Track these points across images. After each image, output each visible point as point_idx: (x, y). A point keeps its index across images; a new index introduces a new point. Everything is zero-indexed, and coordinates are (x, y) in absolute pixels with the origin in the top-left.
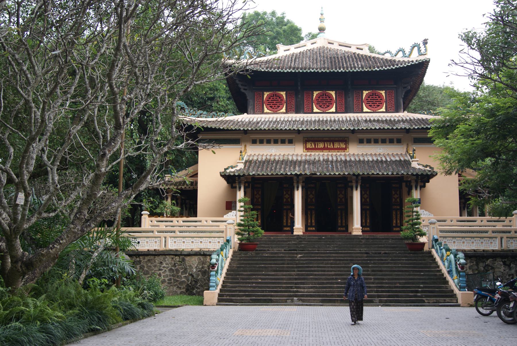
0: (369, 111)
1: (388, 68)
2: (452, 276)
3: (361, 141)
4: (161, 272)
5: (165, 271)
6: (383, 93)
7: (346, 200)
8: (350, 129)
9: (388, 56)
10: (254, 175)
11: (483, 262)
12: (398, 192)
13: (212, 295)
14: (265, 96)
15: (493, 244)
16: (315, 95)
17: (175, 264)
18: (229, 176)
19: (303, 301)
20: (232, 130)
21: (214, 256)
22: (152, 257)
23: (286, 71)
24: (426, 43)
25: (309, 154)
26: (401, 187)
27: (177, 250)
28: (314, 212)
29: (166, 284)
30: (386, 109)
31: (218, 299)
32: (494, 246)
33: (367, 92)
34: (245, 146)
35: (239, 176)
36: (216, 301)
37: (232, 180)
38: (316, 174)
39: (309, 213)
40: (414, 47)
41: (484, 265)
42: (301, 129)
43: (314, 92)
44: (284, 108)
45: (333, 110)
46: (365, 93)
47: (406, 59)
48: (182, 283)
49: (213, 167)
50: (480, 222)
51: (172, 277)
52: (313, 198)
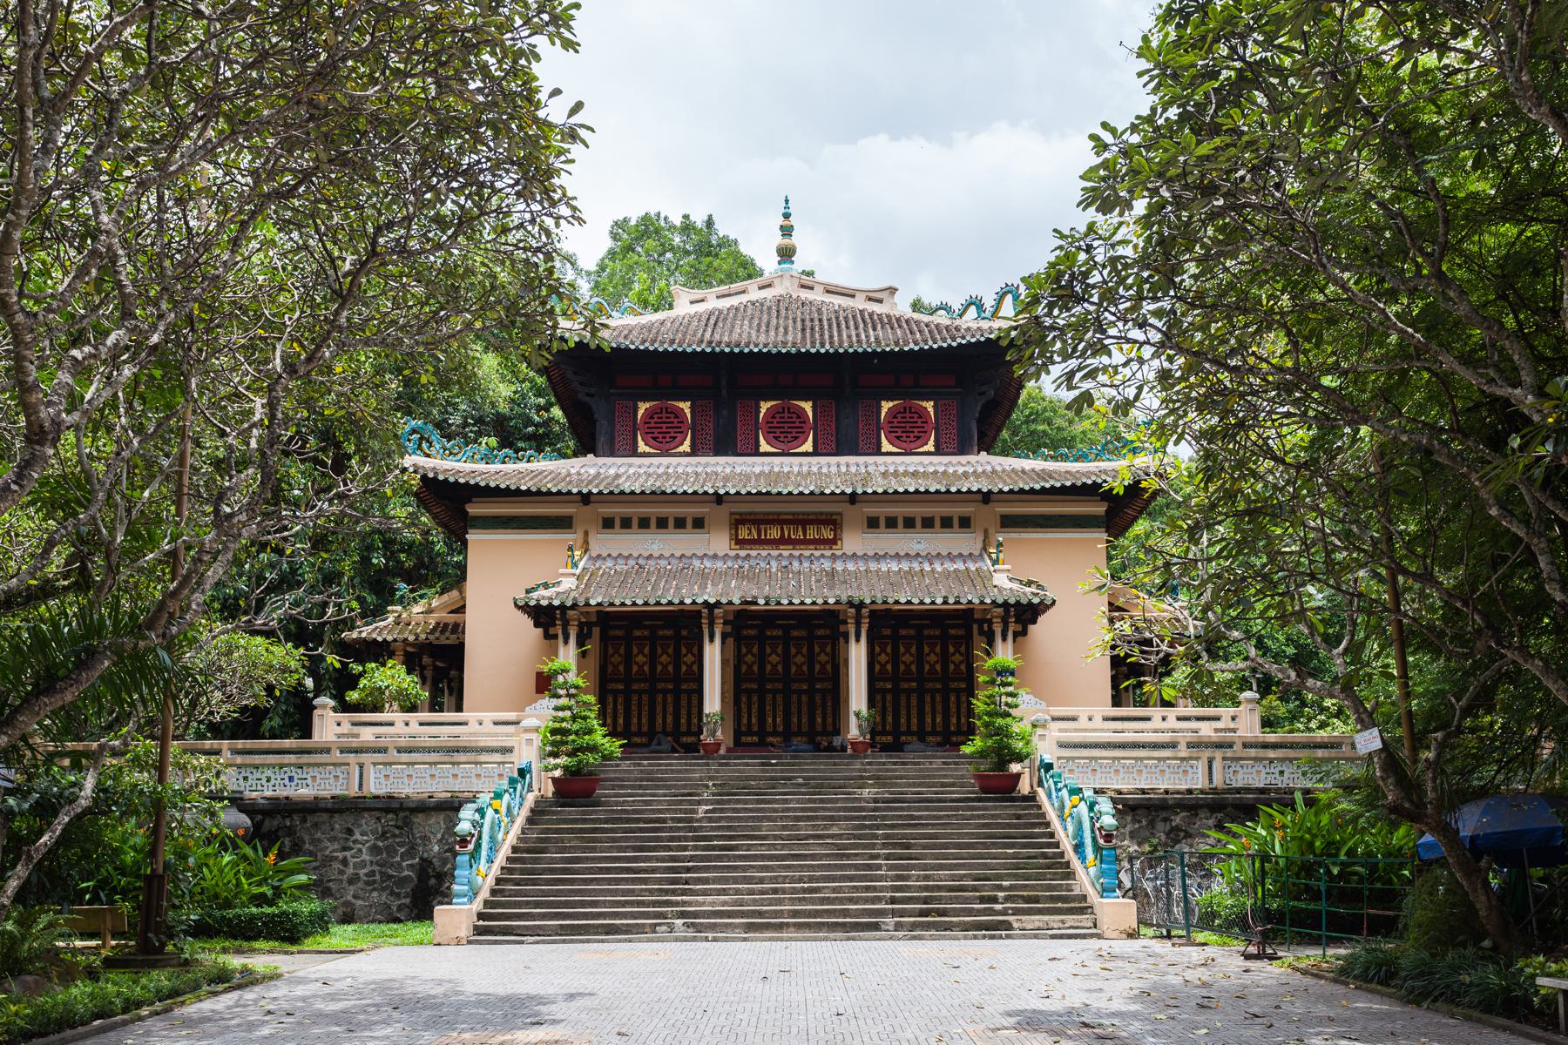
0: (896, 450)
1: (940, 343)
2: (1083, 859)
3: (873, 523)
4: (348, 854)
5: (360, 850)
6: (929, 406)
7: (836, 668)
8: (843, 493)
9: (942, 318)
10: (599, 604)
11: (1166, 820)
12: (963, 649)
13: (456, 915)
14: (641, 412)
15: (1190, 776)
16: (763, 411)
17: (384, 833)
18: (538, 607)
19: (699, 928)
20: (549, 493)
21: (467, 814)
22: (325, 816)
23: (689, 350)
25: (743, 553)
26: (969, 637)
27: (391, 797)
28: (755, 699)
29: (360, 885)
30: (937, 445)
31: (476, 928)
32: (1195, 779)
33: (891, 404)
34: (586, 534)
35: (562, 607)
36: (465, 931)
37: (546, 617)
38: (756, 603)
40: (1005, 294)
41: (1168, 827)
42: (722, 492)
44: (687, 442)
45: (808, 446)
47: (985, 325)
48: (402, 881)
49: (502, 583)
50: (1160, 723)
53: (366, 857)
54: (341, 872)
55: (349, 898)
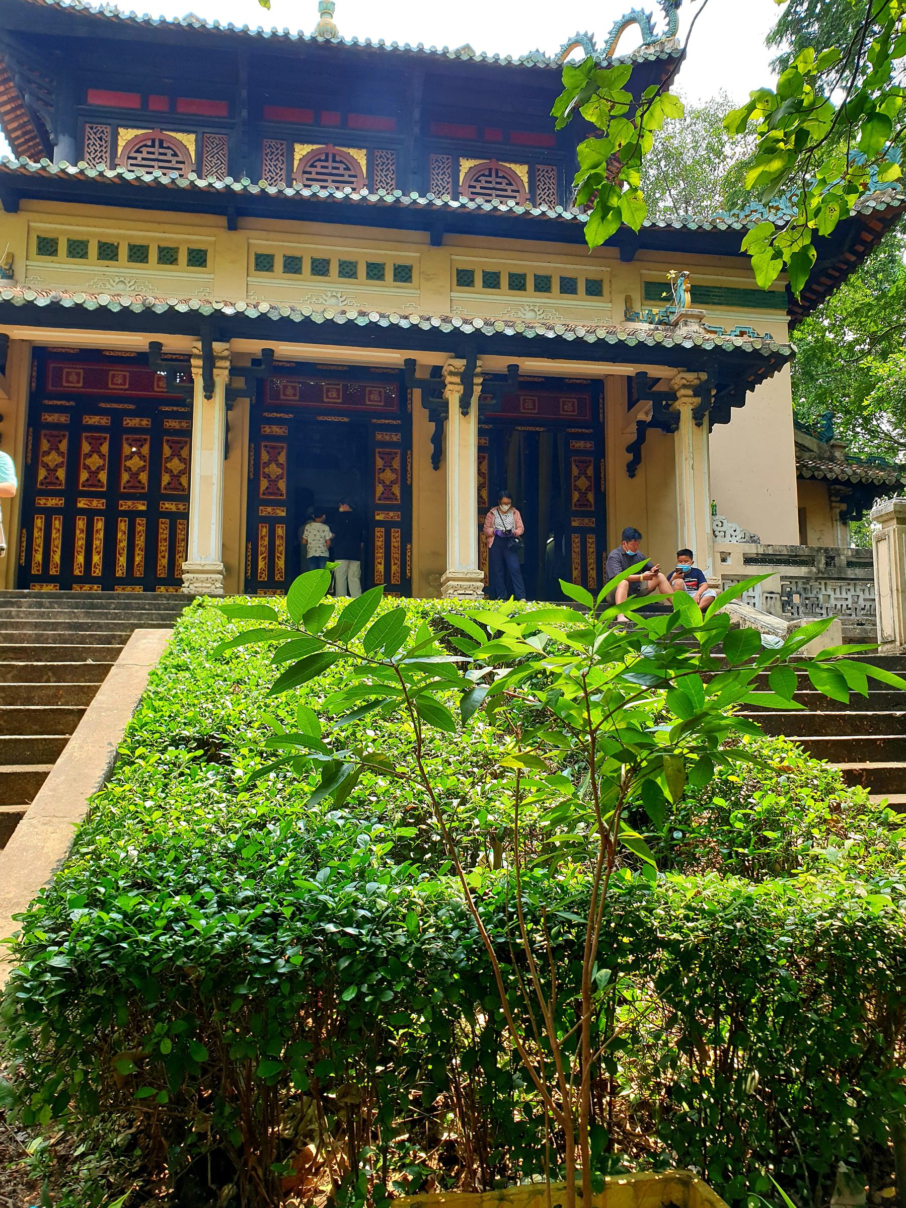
16: (297, 157)
39: (264, 531)
43: (298, 147)
46: (466, 165)
52: (280, 477)
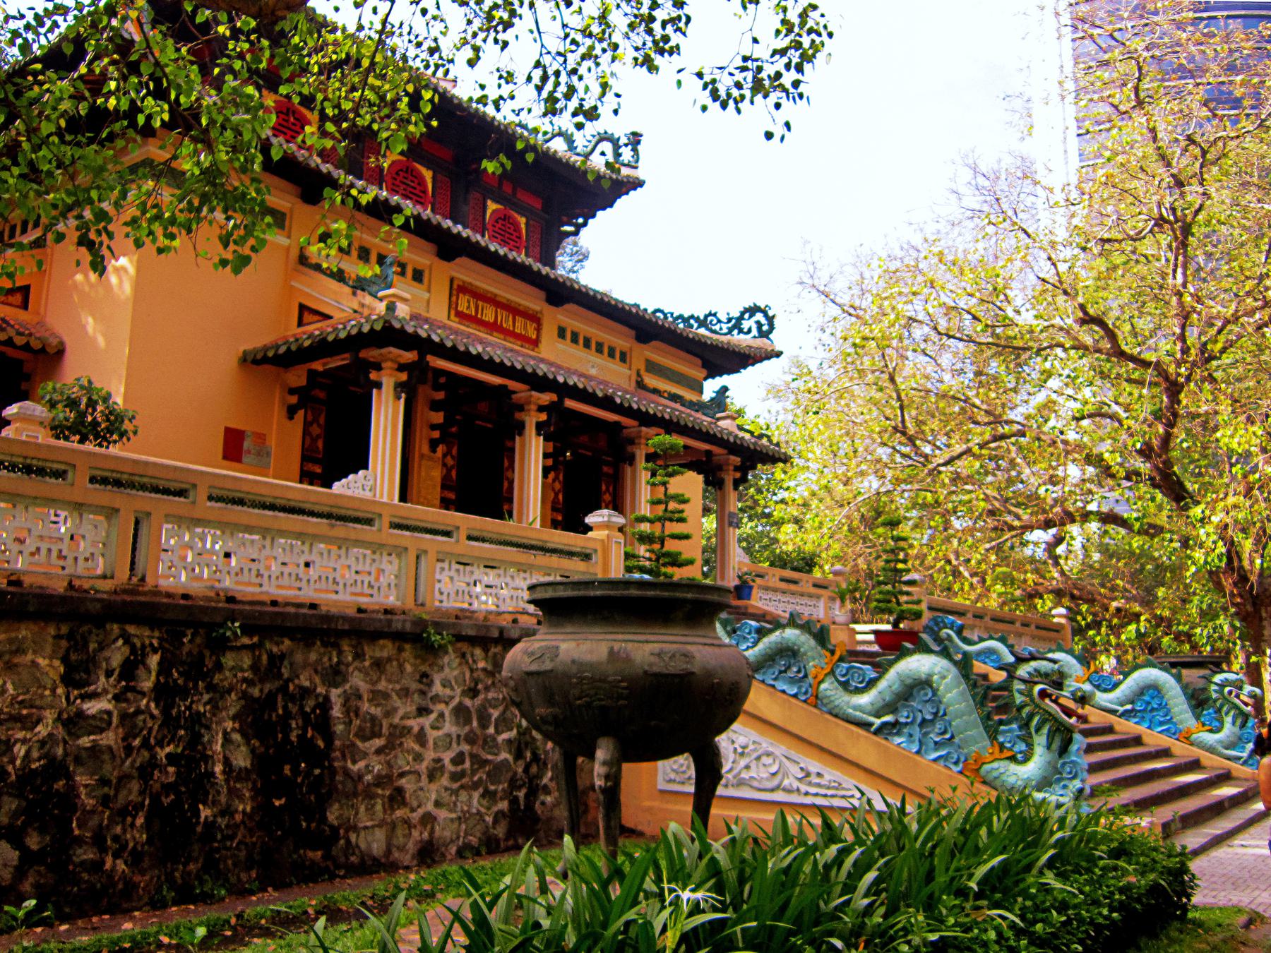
4: (427, 721)
5: (442, 715)
24: (638, 142)
29: (445, 781)
51: (466, 748)
53: (449, 727)
54: (418, 758)
55: (430, 807)
